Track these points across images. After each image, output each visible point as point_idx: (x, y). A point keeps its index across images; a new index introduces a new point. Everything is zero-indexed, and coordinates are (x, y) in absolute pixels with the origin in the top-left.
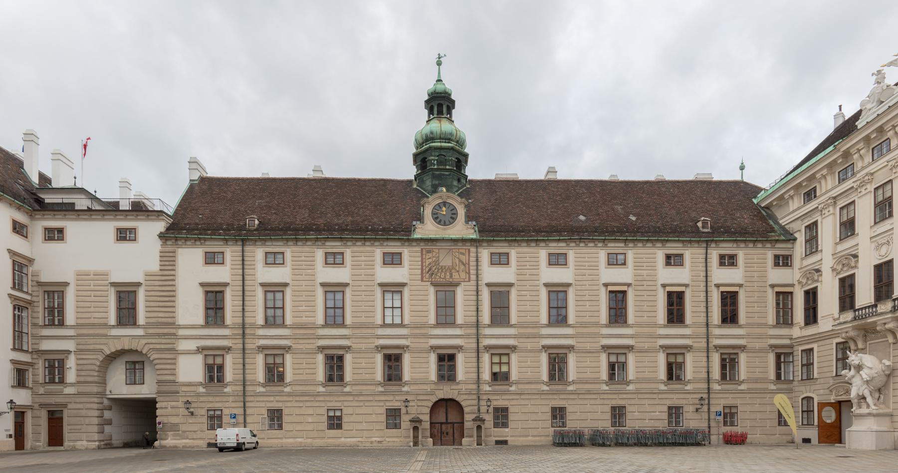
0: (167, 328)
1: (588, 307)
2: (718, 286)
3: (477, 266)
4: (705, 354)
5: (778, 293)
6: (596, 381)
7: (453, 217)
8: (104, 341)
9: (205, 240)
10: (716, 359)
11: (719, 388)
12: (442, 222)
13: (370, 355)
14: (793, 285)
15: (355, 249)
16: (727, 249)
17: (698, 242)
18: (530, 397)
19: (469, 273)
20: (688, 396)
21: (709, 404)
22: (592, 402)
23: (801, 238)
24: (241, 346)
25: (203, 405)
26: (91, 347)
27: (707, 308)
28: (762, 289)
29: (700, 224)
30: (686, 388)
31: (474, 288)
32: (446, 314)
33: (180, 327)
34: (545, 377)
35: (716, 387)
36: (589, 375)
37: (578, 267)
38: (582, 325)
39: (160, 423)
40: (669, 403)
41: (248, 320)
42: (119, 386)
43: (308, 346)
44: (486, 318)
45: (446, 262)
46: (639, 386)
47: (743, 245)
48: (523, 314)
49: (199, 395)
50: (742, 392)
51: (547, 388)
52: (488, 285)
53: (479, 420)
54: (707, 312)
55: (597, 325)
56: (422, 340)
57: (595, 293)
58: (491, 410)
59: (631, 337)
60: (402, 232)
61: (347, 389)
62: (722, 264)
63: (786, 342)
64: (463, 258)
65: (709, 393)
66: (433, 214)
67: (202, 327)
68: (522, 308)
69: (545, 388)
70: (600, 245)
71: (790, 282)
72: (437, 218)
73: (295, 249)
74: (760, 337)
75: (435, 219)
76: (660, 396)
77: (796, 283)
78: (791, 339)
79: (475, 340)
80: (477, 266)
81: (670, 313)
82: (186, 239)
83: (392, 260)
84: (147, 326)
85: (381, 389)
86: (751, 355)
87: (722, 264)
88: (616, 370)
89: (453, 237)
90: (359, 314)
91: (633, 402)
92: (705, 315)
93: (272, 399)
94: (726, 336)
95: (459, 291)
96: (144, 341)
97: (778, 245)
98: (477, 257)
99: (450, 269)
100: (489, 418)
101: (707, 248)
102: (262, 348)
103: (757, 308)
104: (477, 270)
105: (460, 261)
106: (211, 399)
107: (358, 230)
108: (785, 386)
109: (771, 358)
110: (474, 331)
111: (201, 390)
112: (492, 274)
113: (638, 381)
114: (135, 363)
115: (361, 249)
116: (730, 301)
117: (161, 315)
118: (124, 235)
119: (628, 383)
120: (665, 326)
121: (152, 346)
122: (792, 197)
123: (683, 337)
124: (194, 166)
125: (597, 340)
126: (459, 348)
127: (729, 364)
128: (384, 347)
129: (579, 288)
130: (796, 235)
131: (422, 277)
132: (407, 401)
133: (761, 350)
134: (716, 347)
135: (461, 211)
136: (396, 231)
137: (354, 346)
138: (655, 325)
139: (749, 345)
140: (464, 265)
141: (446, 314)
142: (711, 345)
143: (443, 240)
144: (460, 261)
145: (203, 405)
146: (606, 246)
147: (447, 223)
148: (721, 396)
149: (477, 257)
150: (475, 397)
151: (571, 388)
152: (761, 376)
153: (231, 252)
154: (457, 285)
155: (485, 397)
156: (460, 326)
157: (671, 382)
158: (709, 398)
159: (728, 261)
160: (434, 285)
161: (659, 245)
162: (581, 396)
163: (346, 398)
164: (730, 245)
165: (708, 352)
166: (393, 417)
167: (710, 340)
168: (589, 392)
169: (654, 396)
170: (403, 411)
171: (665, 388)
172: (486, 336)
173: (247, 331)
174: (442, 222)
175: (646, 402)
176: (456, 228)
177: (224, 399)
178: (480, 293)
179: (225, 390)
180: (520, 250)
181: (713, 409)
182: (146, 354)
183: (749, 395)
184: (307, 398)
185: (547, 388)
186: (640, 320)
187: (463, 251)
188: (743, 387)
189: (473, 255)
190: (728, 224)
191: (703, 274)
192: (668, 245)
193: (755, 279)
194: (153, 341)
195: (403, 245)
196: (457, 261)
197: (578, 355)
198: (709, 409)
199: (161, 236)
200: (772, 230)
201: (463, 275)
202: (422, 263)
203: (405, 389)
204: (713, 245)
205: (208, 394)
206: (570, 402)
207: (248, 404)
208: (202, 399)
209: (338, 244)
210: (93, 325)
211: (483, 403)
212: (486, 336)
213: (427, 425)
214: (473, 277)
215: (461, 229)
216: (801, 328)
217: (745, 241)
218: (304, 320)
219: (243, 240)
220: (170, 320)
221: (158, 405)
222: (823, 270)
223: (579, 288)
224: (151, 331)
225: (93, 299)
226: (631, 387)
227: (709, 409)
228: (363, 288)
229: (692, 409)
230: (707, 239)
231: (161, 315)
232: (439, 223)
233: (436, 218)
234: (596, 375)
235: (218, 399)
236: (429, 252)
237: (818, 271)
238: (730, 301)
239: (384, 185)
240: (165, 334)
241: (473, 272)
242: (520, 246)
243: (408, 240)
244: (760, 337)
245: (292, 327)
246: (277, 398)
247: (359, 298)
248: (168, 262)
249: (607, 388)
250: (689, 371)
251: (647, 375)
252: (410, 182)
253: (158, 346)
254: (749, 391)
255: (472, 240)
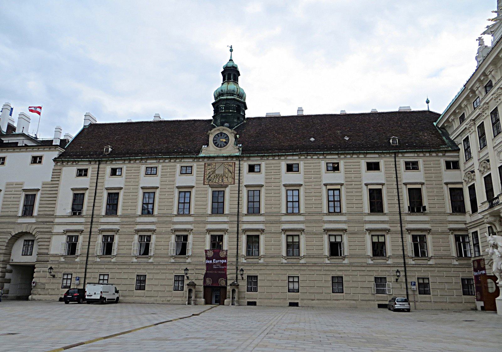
0: (49, 218)
1: (314, 201)
2: (405, 184)
3: (239, 173)
4: (400, 236)
5: (451, 189)
6: (321, 256)
7: (226, 143)
8: (12, 226)
9: (79, 161)
10: (409, 239)
11: (413, 262)
12: (219, 146)
13: (167, 236)
14: (462, 183)
15: (164, 164)
16: (411, 157)
17: (389, 153)
18: (273, 268)
19: (234, 179)
20: (389, 269)
21: (406, 276)
22: (318, 272)
23: (461, 147)
24: (89, 230)
25: (61, 270)
26: (5, 230)
27: (399, 200)
28: (438, 186)
29: (391, 141)
30: (388, 262)
31: (237, 189)
32: (218, 208)
33: (56, 217)
34: (284, 254)
35: (410, 262)
36: (315, 252)
37: (306, 173)
38: (310, 214)
39: (34, 283)
40: (376, 274)
41: (95, 212)
42: (18, 256)
43: (129, 230)
44: (244, 210)
45: (220, 171)
46: (352, 260)
47: (421, 155)
48: (269, 206)
49: (60, 263)
50: (431, 266)
51: (285, 261)
52: (246, 186)
53: (235, 285)
54: (399, 204)
55: (321, 214)
56: (201, 225)
57: (319, 190)
58: (245, 277)
59: (345, 222)
60: (193, 152)
61: (151, 260)
62: (407, 168)
63: (463, 226)
64: (230, 168)
65: (405, 267)
66: (214, 140)
67: (69, 217)
68: (269, 202)
69: (284, 261)
70: (321, 157)
71: (460, 181)
72: (216, 143)
73: (129, 165)
74: (441, 222)
75: (215, 144)
76: (368, 269)
77: (463, 181)
78: (466, 224)
79: (236, 225)
80: (239, 173)
81: (372, 204)
82: (68, 162)
83: (187, 171)
84: (39, 216)
85: (173, 261)
86: (435, 236)
87: (407, 168)
88: (335, 249)
89: (225, 155)
90: (162, 208)
91: (348, 273)
92: (398, 206)
93: (103, 267)
94: (416, 222)
95: (227, 191)
96: (34, 226)
97: (447, 154)
98: (240, 167)
99: (222, 176)
100: (243, 284)
101: (395, 157)
102: (102, 231)
103: (437, 200)
104: (239, 176)
105: (229, 170)
106: (66, 266)
107: (168, 153)
108: (465, 262)
109: (452, 238)
110: (235, 218)
111: (62, 259)
112: (249, 179)
113: (351, 256)
114: (28, 239)
115: (168, 164)
116: (415, 195)
117: (47, 209)
118: (36, 160)
119: (344, 258)
120: (369, 214)
121: (38, 230)
122: (453, 120)
123: (383, 222)
124: (88, 117)
125: (320, 225)
126: (225, 231)
127: (419, 242)
128: (176, 230)
129: (307, 187)
130: (460, 146)
131: (204, 182)
132: (186, 269)
133: (443, 233)
134: (408, 230)
135: (232, 139)
136: (190, 153)
137: (158, 230)
138: (362, 214)
139: (433, 229)
140: (231, 173)
141: (218, 208)
142: (404, 229)
143: (218, 157)
144: (229, 170)
145: (61, 270)
146: (325, 158)
147: (222, 145)
148: (415, 269)
149: (240, 167)
150: (235, 267)
151: (302, 261)
152: (445, 253)
153: (92, 168)
154: (226, 186)
155: (240, 268)
156: (227, 215)
157: (375, 258)
158: (405, 271)
159: (412, 166)
160: (211, 186)
161: (362, 156)
162: (310, 268)
163: (150, 267)
164: (412, 155)
165: (402, 234)
166: (179, 279)
167: (403, 225)
168: (315, 264)
169: (363, 269)
170: (185, 278)
171: (372, 262)
172: (244, 222)
173: (94, 220)
174: (219, 146)
175: (359, 273)
176: (228, 149)
177: (74, 266)
178: (240, 192)
179: (76, 260)
180: (268, 162)
181: (409, 280)
182: (34, 235)
183: (437, 269)
184: (125, 267)
185: (285, 261)
186: (350, 210)
187: (231, 164)
188: (431, 262)
189: (237, 166)
190: (413, 140)
191: (394, 176)
192: (368, 156)
193: (433, 179)
194: (40, 226)
195: (194, 161)
196: (227, 170)
197: (307, 236)
198: (406, 280)
199: (55, 160)
200: (444, 143)
201: (230, 180)
202: (205, 172)
203: (189, 260)
204: (400, 155)
205: (65, 263)
206: (302, 272)
207: (88, 270)
208: (61, 266)
209: (155, 161)
210: (9, 216)
211: (239, 272)
212: (244, 222)
213: (202, 289)
214: (237, 181)
215: (232, 149)
216: (470, 215)
217: (422, 152)
218: (129, 212)
219: (99, 161)
220: (51, 213)
221: (35, 270)
222: (475, 171)
223: (307, 187)
224: (40, 220)
225: (12, 199)
226: (346, 261)
227: (406, 280)
228: (167, 190)
229: (393, 279)
230: (395, 151)
231: (47, 209)
232: (217, 146)
233: (215, 144)
234: (320, 252)
235: (70, 266)
236: (209, 165)
237: (473, 172)
238: (415, 195)
239: (193, 124)
240: (47, 222)
241: (237, 177)
242: (268, 159)
243: (196, 158)
244: (441, 222)
245: (121, 217)
246: (106, 266)
247: (163, 197)
248: (56, 175)
249: (329, 262)
250: (389, 250)
251: (357, 252)
252: (210, 121)
253: (42, 230)
254: (436, 266)
255: (236, 156)
